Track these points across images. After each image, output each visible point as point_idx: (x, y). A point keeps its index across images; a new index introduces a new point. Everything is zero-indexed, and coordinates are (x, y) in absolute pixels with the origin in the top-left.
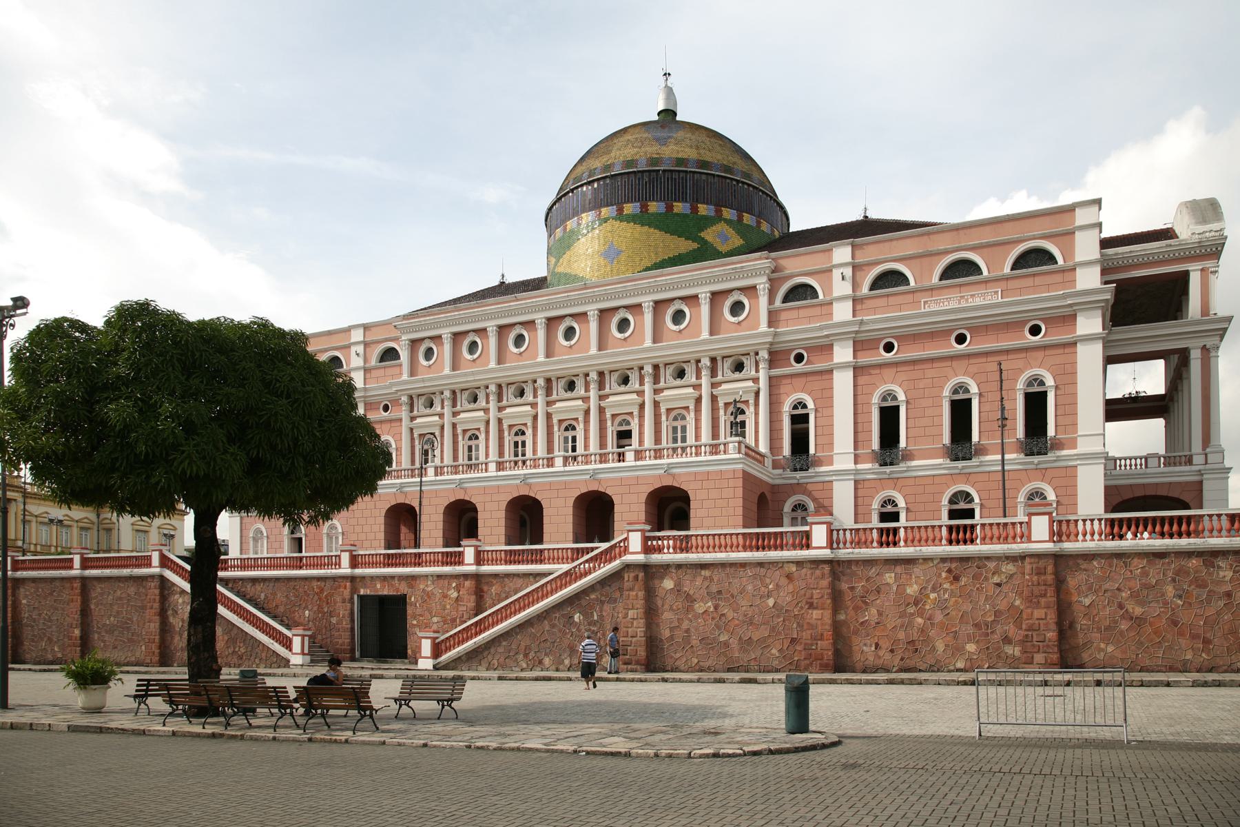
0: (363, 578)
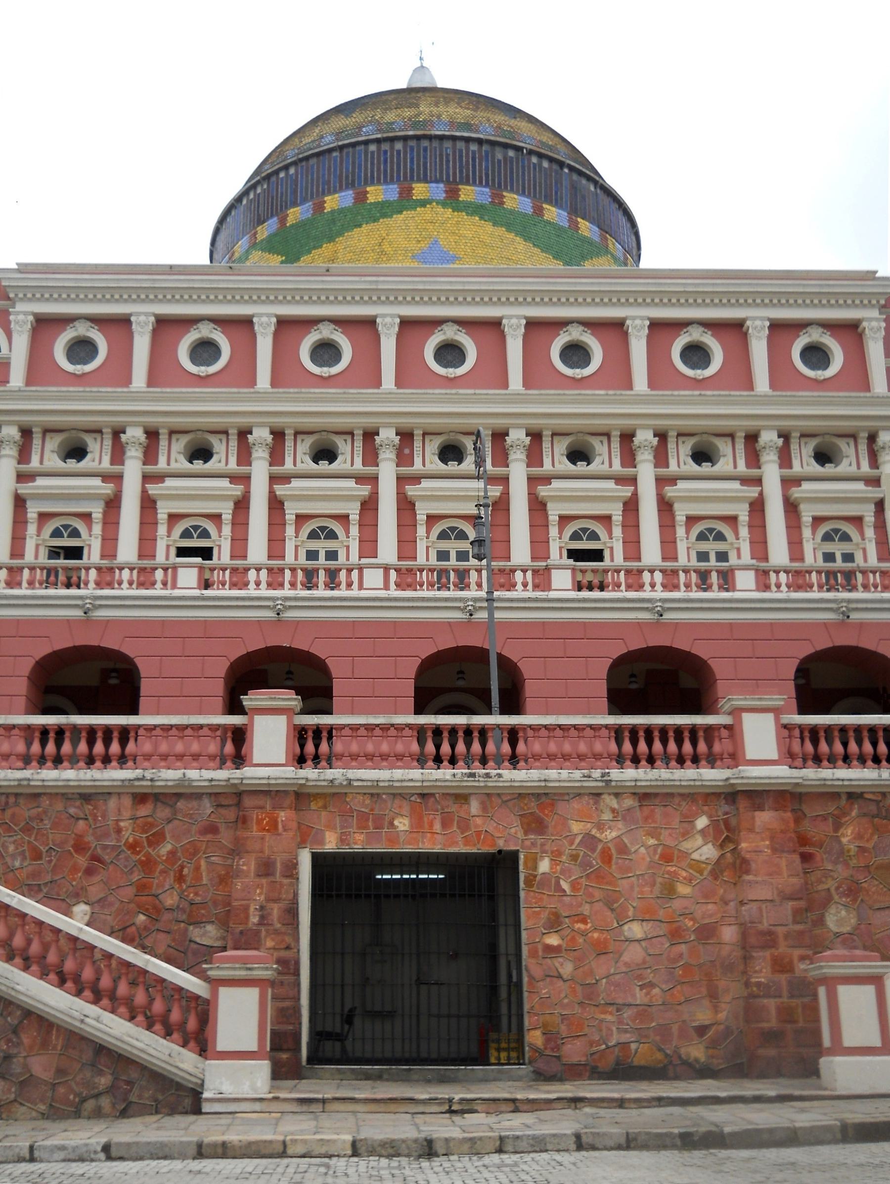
0: (334, 797)
